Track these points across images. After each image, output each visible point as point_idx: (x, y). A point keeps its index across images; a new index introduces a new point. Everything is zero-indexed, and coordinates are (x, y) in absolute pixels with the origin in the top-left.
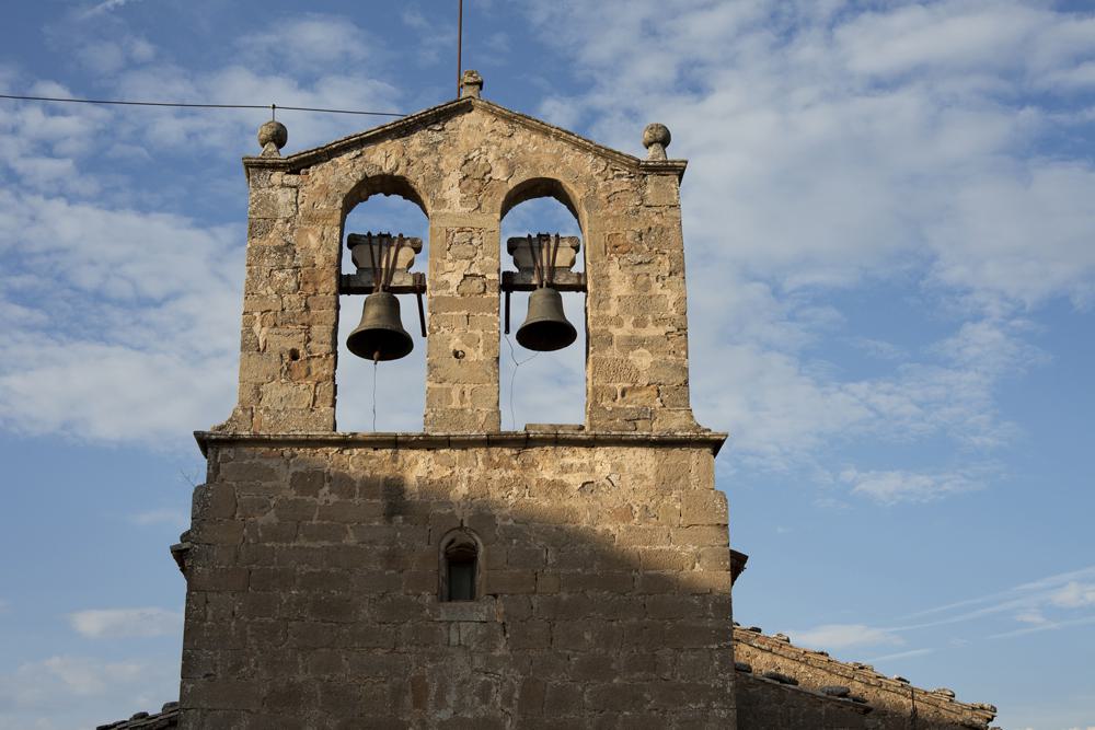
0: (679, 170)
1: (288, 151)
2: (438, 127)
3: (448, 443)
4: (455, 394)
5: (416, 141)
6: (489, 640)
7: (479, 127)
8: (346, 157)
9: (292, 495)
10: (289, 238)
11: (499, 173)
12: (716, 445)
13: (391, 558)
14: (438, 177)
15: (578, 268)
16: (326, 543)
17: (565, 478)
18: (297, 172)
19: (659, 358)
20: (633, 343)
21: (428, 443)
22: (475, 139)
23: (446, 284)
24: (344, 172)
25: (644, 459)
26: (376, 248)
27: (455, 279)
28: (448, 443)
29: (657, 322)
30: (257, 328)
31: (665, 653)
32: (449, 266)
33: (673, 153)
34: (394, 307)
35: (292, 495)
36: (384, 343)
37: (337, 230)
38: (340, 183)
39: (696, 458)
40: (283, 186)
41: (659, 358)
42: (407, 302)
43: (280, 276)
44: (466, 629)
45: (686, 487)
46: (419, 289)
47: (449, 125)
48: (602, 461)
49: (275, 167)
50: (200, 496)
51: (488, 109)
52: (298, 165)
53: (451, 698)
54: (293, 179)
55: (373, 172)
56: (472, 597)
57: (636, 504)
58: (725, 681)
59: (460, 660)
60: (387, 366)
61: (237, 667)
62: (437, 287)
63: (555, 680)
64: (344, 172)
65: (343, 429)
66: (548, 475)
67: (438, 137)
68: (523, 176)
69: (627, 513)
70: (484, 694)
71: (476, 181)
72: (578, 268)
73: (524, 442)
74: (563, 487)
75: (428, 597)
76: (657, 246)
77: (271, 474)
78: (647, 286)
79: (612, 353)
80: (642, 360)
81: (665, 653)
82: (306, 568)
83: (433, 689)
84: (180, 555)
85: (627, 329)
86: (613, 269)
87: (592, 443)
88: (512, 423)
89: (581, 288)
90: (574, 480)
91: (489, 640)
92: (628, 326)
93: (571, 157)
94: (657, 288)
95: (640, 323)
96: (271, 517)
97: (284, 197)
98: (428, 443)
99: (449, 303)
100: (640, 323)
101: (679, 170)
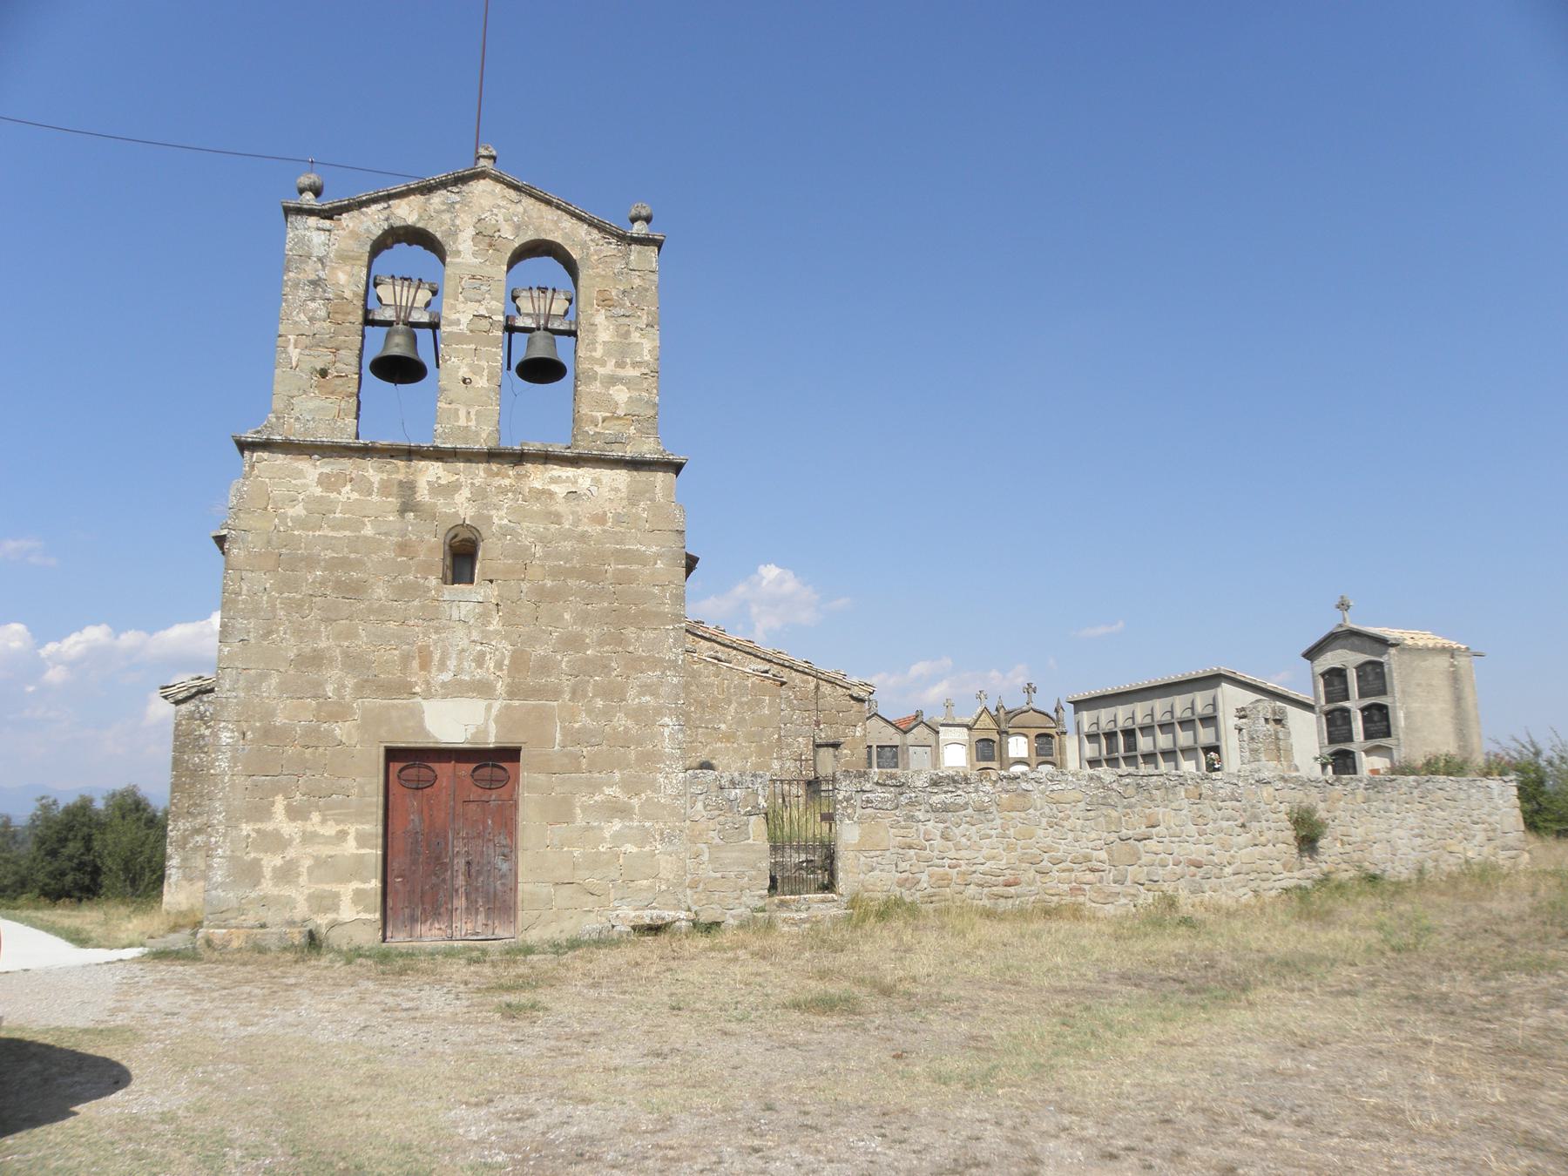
2: (455, 189)
4: (462, 413)
5: (437, 198)
6: (484, 617)
7: (492, 192)
8: (374, 207)
9: (318, 491)
10: (321, 274)
13: (403, 548)
14: (454, 233)
16: (347, 533)
17: (553, 487)
18: (331, 218)
19: (635, 394)
20: (613, 380)
22: (486, 202)
23: (458, 323)
26: (398, 289)
27: (465, 319)
29: (635, 365)
30: (291, 347)
31: (630, 632)
32: (461, 307)
37: (365, 271)
38: (368, 230)
39: (660, 478)
40: (318, 229)
41: (635, 394)
43: (312, 305)
44: (465, 609)
45: (652, 500)
47: (465, 188)
48: (584, 477)
53: (452, 663)
54: (327, 224)
55: (398, 223)
56: (472, 582)
58: (677, 655)
59: (461, 632)
61: (270, 633)
62: (451, 323)
63: (540, 651)
64: (372, 221)
66: (538, 485)
67: (457, 198)
68: (529, 235)
69: (600, 519)
70: (480, 661)
71: (486, 237)
74: (551, 494)
75: (433, 581)
78: (628, 333)
79: (596, 387)
81: (630, 632)
82: (329, 554)
83: (437, 656)
85: (610, 368)
90: (560, 490)
91: (484, 617)
92: (611, 363)
93: (568, 223)
94: (635, 337)
95: (620, 365)
96: (299, 510)
97: (318, 238)
99: (460, 338)
100: (620, 365)
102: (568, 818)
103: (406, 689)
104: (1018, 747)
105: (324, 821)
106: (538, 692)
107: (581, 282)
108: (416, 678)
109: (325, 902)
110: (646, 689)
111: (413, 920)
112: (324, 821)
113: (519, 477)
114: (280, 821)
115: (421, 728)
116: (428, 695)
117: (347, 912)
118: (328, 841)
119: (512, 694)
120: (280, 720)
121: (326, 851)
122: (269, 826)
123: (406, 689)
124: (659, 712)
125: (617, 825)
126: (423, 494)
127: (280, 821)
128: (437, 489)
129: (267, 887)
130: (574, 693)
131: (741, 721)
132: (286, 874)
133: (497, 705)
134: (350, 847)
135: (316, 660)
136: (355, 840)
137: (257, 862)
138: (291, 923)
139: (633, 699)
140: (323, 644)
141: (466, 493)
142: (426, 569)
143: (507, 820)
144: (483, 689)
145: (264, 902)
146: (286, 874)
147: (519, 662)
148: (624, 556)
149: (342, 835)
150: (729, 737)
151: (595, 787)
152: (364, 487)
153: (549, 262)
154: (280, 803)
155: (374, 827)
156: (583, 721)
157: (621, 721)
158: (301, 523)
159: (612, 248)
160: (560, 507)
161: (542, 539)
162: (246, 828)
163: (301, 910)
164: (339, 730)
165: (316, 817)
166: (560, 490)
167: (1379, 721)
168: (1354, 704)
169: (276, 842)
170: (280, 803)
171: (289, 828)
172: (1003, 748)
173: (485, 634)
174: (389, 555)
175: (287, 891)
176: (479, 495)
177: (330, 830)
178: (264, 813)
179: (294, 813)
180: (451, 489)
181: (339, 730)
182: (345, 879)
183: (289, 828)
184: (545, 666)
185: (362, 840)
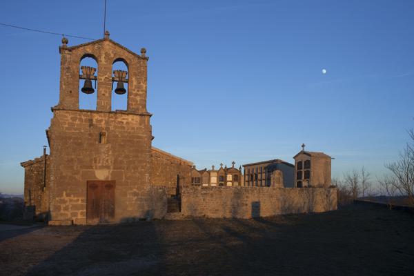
0: (146, 59)
1: (69, 46)
3: (101, 112)
9: (70, 121)
11: (112, 55)
12: (151, 116)
13: (90, 135)
14: (100, 56)
15: (127, 78)
20: (136, 95)
21: (97, 112)
22: (108, 47)
24: (81, 52)
25: (137, 118)
28: (101, 112)
29: (142, 91)
31: (139, 155)
33: (146, 55)
34: (91, 83)
35: (70, 121)
36: (89, 90)
39: (147, 118)
42: (93, 82)
43: (67, 74)
46: (95, 79)
48: (130, 118)
49: (66, 49)
50: (52, 120)
51: (111, 41)
52: (70, 50)
57: (136, 126)
59: (103, 155)
63: (120, 159)
65: (81, 108)
66: (120, 120)
68: (118, 57)
69: (133, 128)
70: (107, 161)
72: (127, 78)
73: (116, 113)
74: (123, 123)
75: (97, 143)
76: (142, 75)
77: (66, 117)
78: (140, 83)
79: (132, 96)
80: (138, 98)
81: (139, 155)
82: (73, 136)
83: (98, 160)
84: (47, 132)
86: (134, 79)
88: (113, 109)
89: (127, 82)
90: (125, 121)
91: (108, 151)
93: (127, 54)
95: (138, 91)
96: (67, 126)
97: (68, 56)
99: (102, 83)
100: (138, 91)
101: (146, 59)
102: (126, 196)
103: (91, 167)
104: (230, 177)
105: (74, 197)
106: (120, 168)
107: (130, 67)
108: (93, 164)
109: (75, 214)
110: (143, 167)
111: (93, 218)
112: (74, 197)
113: (116, 118)
114: (64, 197)
115: (95, 177)
116: (96, 168)
117: (79, 217)
118: (75, 201)
120: (64, 174)
121: (75, 203)
122: (62, 198)
125: (136, 197)
126: (94, 122)
127: (64, 197)
128: (97, 121)
129: (62, 211)
131: (162, 172)
134: (80, 202)
136: (81, 201)
137: (60, 206)
138: (68, 220)
139: (139, 169)
140: (73, 157)
141: (104, 122)
144: (108, 167)
145: (62, 214)
146: (66, 209)
147: (116, 161)
148: (138, 137)
149: (78, 200)
153: (122, 62)
155: (85, 198)
156: (129, 174)
157: (137, 175)
158: (67, 128)
159: (136, 60)
162: (57, 199)
163: (69, 216)
164: (77, 177)
165: (72, 196)
166: (125, 121)
167: (308, 175)
168: (303, 170)
169: (64, 202)
171: (67, 199)
172: (226, 177)
174: (87, 136)
175: (66, 212)
176: (107, 123)
177: (76, 199)
178: (62, 196)
179: (67, 195)
180: (101, 121)
181: (77, 177)
182: (79, 210)
183: (67, 199)
184: (121, 162)
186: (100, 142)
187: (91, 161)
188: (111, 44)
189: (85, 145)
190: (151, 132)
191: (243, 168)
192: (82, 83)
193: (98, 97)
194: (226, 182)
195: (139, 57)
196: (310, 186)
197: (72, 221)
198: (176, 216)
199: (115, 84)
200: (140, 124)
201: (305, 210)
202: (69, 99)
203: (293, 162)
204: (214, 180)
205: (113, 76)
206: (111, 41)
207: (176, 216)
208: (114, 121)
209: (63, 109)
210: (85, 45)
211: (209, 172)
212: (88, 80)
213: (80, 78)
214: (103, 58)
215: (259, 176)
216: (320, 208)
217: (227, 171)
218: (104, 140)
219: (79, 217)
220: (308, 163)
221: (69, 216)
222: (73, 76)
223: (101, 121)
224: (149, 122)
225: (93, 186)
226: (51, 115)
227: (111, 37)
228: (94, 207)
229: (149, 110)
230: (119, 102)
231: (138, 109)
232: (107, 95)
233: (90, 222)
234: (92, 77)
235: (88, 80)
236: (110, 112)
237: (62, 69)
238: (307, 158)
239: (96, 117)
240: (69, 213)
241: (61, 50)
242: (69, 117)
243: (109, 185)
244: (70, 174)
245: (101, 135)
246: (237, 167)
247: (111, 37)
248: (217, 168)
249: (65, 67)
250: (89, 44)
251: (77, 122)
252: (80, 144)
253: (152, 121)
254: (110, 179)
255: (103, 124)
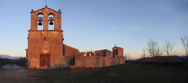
0: (61, 13)
5: (43, 10)
11: (48, 12)
12: (63, 31)
13: (41, 38)
24: (37, 12)
25: (58, 32)
36: (40, 24)
39: (61, 32)
42: (42, 22)
46: (43, 20)
48: (55, 32)
50: (28, 35)
52: (34, 12)
60: (41, 26)
65: (38, 30)
66: (51, 33)
68: (50, 13)
69: (56, 36)
73: (50, 31)
76: (59, 18)
87: (54, 31)
89: (54, 21)
90: (53, 33)
91: (47, 44)
93: (53, 11)
96: (33, 36)
97: (33, 14)
98: (43, 31)
101: (61, 13)
103: (41, 49)
104: (90, 55)
106: (52, 49)
109: (36, 65)
111: (42, 66)
114: (33, 59)
115: (43, 52)
119: (50, 49)
121: (36, 61)
123: (41, 49)
124: (61, 51)
125: (58, 60)
126: (42, 34)
128: (43, 34)
129: (32, 64)
130: (54, 50)
131: (68, 52)
132: (33, 63)
133: (48, 50)
134: (38, 61)
135: (35, 47)
136: (38, 60)
139: (58, 50)
142: (43, 40)
143: (49, 59)
144: (47, 49)
145: (32, 65)
146: (33, 63)
147: (50, 47)
148: (58, 39)
150: (67, 53)
151: (56, 57)
152: (38, 34)
154: (33, 58)
155: (39, 59)
159: (57, 13)
160: (53, 35)
161: (52, 37)
166: (53, 33)
170: (33, 58)
171: (33, 59)
172: (89, 55)
173: (47, 45)
176: (47, 34)
177: (36, 60)
178: (32, 58)
179: (33, 58)
180: (45, 34)
183: (33, 59)
184: (52, 47)
185: (38, 60)
186: (45, 41)
187: (41, 47)
188: (48, 9)
189: (39, 42)
190: (63, 37)
191: (94, 52)
192: (38, 22)
193: (44, 26)
194: (89, 56)
195: (58, 12)
196: (118, 57)
197: (35, 67)
198: (72, 67)
199: (50, 22)
200: (59, 34)
201: (118, 64)
202: (34, 28)
203: (112, 51)
204: (85, 55)
205: (49, 19)
206: (48, 8)
207: (72, 67)
208: (49, 34)
209: (32, 31)
210: (39, 10)
211: (84, 53)
212: (40, 21)
213: (38, 21)
214: (45, 14)
215: (100, 54)
216: (121, 63)
217: (90, 53)
218: (46, 40)
219: (38, 66)
220: (117, 50)
221: (34, 65)
222: (35, 20)
223: (44, 34)
224: (62, 33)
225: (42, 55)
226: (28, 33)
227: (47, 7)
228: (42, 64)
229: (62, 29)
230: (51, 27)
231: (58, 29)
232: (47, 25)
233: (41, 68)
234: (41, 20)
235: (40, 21)
236: (48, 31)
237: (31, 18)
238: (117, 48)
239: (43, 32)
240: (34, 64)
241: (31, 12)
242: (34, 33)
243: (48, 55)
244: (34, 51)
245: (45, 39)
246: (93, 52)
247: (47, 7)
248: (86, 52)
249: (32, 18)
250: (40, 10)
251: (37, 34)
252: (37, 42)
253: (63, 33)
254: (48, 53)
255: (45, 35)
